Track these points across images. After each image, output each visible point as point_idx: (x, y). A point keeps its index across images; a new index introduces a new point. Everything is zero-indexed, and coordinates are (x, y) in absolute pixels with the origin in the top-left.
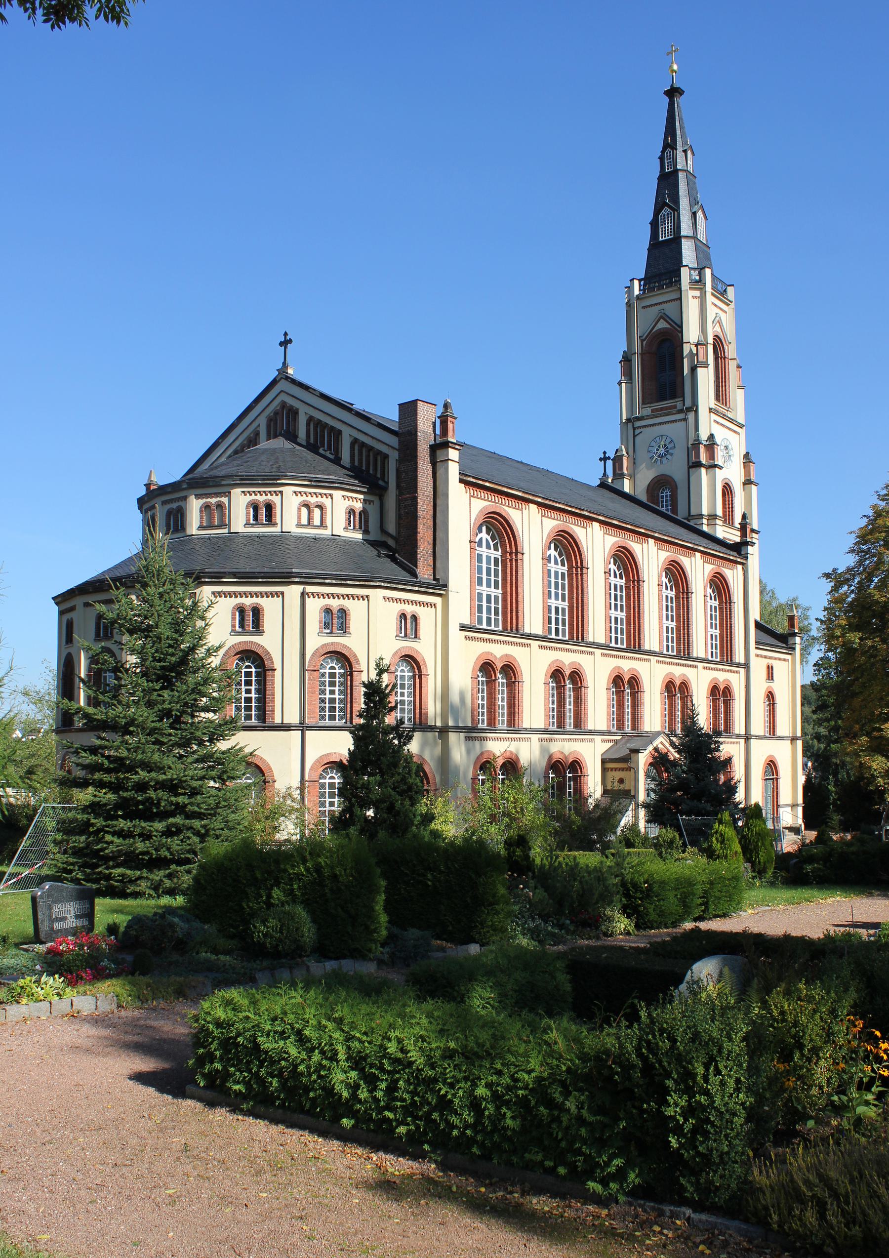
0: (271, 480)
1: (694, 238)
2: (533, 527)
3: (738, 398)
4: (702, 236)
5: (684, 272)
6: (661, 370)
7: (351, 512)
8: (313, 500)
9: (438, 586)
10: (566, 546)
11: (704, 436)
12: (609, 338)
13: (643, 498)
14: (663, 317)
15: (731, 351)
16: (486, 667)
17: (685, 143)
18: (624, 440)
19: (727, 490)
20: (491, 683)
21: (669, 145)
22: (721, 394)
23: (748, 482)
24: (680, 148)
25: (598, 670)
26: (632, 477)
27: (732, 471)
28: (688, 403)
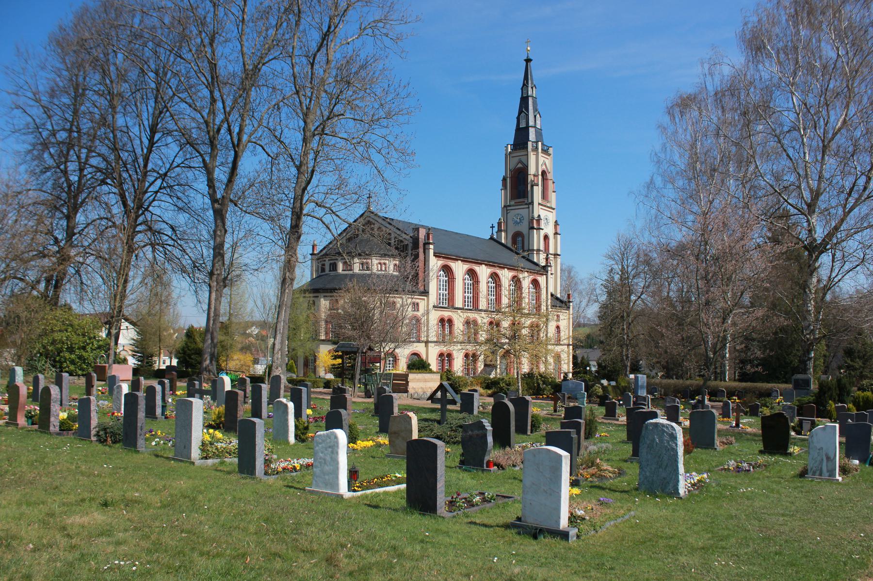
0: (369, 255)
1: (535, 127)
2: (459, 269)
3: (553, 197)
4: (538, 126)
5: (530, 144)
6: (518, 185)
7: (395, 265)
8: (382, 261)
9: (425, 293)
10: (472, 273)
11: (536, 215)
12: (498, 169)
13: (509, 245)
14: (520, 162)
15: (549, 176)
16: (442, 320)
17: (532, 83)
18: (503, 215)
19: (546, 237)
20: (443, 326)
21: (525, 85)
22: (545, 196)
23: (556, 233)
24: (530, 85)
25: (483, 319)
26: (506, 231)
27: (549, 229)
28: (530, 201)
